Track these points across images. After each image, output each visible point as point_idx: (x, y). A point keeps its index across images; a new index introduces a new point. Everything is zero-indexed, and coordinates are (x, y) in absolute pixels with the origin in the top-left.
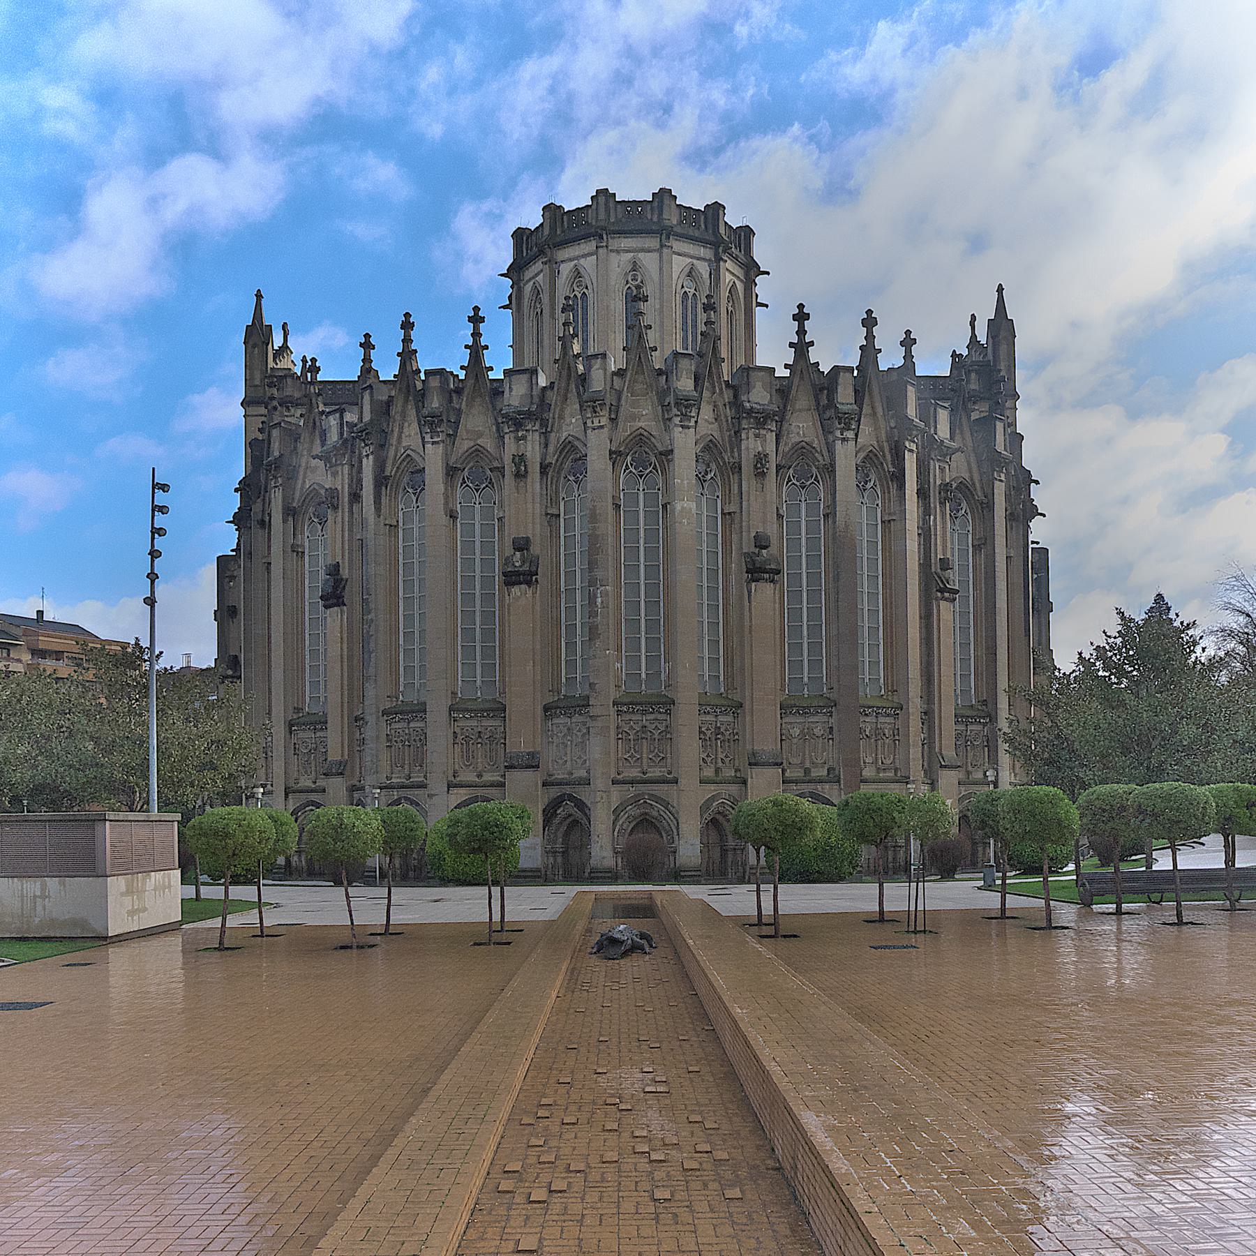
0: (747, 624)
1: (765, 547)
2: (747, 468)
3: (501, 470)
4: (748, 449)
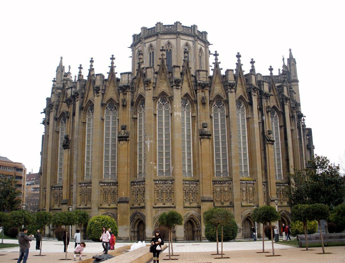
0: (200, 153)
1: (206, 127)
2: (199, 101)
3: (118, 104)
4: (199, 95)
